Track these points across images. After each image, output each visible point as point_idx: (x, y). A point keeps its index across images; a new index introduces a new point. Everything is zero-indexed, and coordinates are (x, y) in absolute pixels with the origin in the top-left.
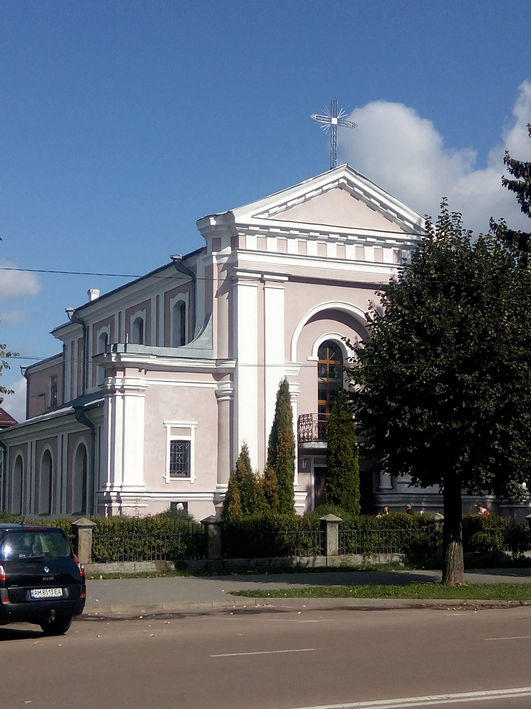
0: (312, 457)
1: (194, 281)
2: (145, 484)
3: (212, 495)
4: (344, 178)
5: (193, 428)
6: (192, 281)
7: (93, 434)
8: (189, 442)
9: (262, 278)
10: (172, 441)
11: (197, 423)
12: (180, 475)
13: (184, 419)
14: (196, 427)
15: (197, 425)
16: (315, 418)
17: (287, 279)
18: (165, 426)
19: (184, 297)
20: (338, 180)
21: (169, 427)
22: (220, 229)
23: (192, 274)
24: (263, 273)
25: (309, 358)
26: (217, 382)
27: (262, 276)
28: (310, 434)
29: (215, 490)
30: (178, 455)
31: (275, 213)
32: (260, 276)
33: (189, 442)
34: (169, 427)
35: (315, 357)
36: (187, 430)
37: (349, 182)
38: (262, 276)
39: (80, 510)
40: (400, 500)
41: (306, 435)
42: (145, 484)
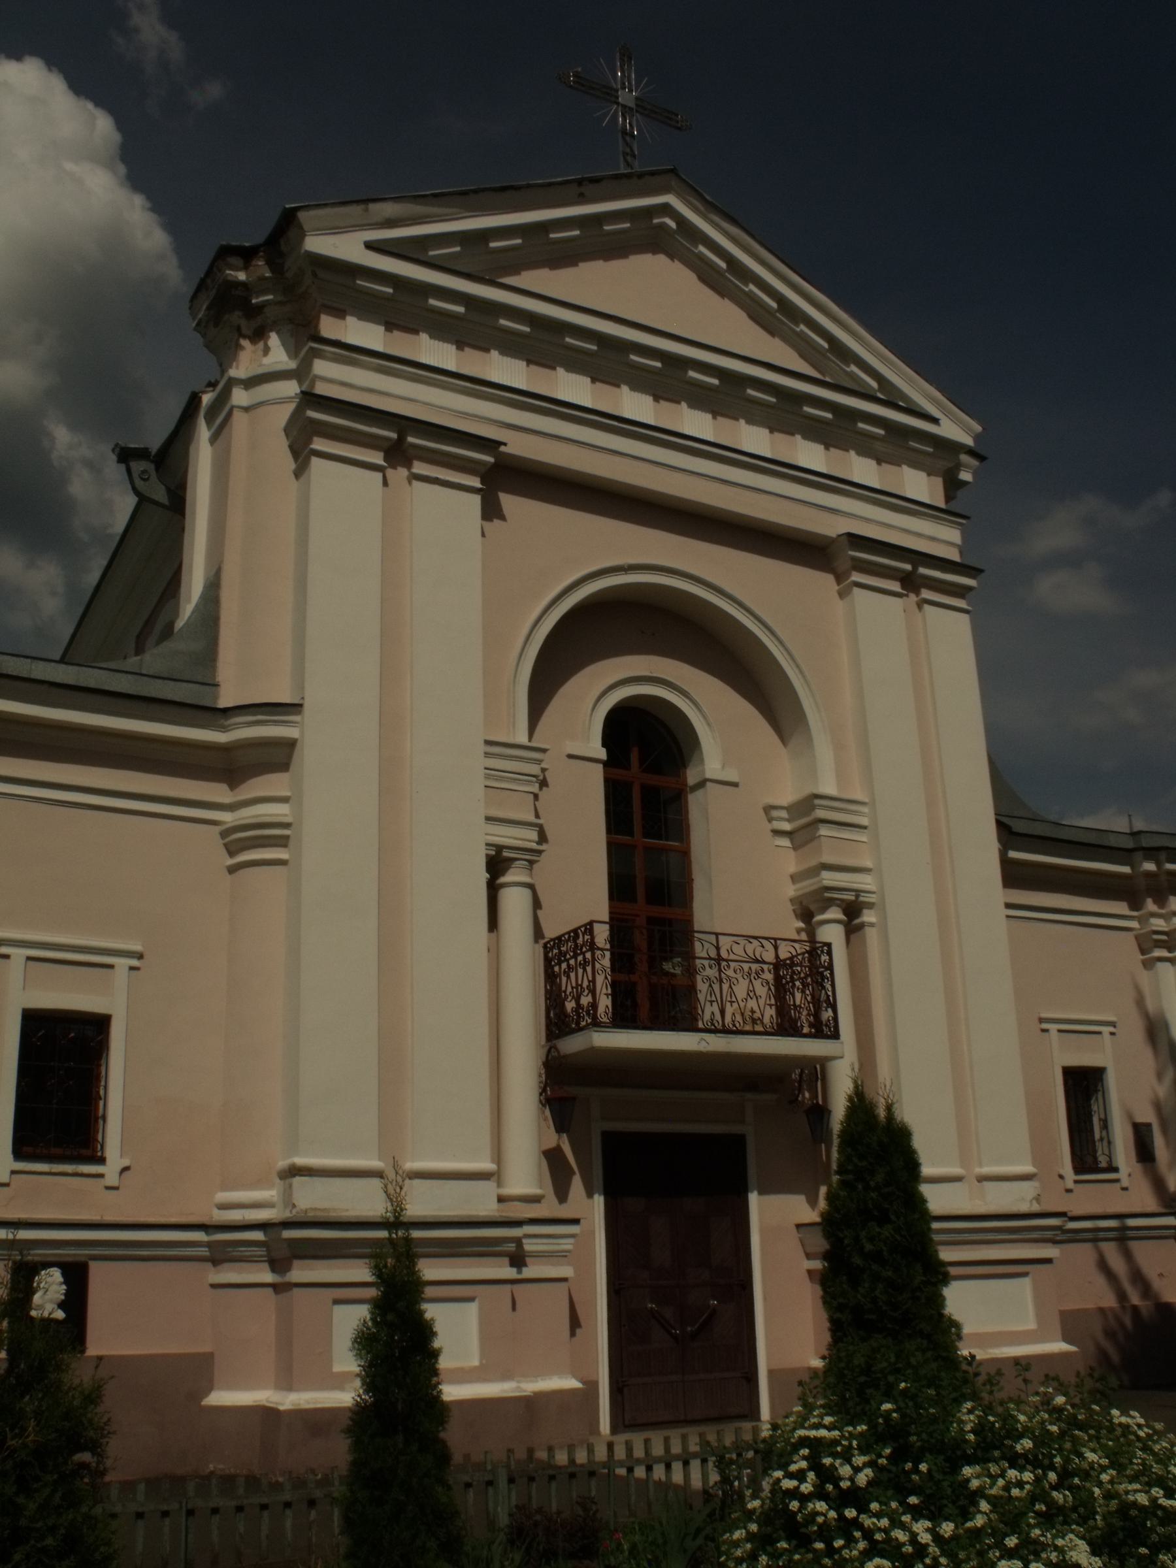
4: (666, 209)
8: (101, 1023)
15: (140, 956)
16: (602, 934)
27: (401, 439)
28: (586, 1000)
33: (101, 1023)
37: (681, 221)
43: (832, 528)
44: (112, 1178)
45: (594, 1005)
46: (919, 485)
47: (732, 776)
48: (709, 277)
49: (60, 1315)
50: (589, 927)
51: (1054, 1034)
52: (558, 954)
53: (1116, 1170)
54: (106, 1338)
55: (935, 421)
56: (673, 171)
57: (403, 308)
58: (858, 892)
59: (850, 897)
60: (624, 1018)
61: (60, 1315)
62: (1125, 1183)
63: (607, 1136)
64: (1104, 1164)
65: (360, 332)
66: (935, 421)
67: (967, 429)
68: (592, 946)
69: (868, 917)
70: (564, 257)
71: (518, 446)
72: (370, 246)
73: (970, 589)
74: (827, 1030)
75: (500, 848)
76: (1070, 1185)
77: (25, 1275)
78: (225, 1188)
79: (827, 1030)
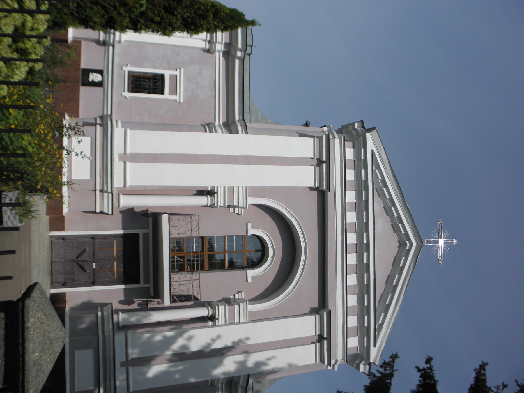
0: (150, 231)
3: (109, 113)
4: (411, 245)
5: (177, 98)
8: (162, 93)
9: (322, 162)
10: (162, 77)
11: (182, 101)
12: (130, 82)
13: (185, 90)
14: (178, 101)
18: (178, 70)
21: (177, 73)
22: (353, 131)
25: (249, 225)
26: (221, 123)
27: (324, 162)
29: (114, 116)
30: (150, 82)
33: (162, 93)
34: (177, 73)
35: (251, 232)
36: (174, 92)
37: (409, 251)
40: (106, 334)
43: (331, 306)
46: (353, 342)
47: (250, 280)
48: (396, 261)
49: (90, 79)
54: (84, 91)
55: (375, 346)
57: (360, 164)
58: (218, 319)
59: (217, 316)
61: (90, 79)
63: (137, 235)
65: (350, 154)
66: (375, 346)
67: (376, 359)
69: (210, 323)
70: (388, 212)
71: (330, 195)
72: (372, 151)
73: (323, 363)
77: (100, 72)
78: (122, 122)
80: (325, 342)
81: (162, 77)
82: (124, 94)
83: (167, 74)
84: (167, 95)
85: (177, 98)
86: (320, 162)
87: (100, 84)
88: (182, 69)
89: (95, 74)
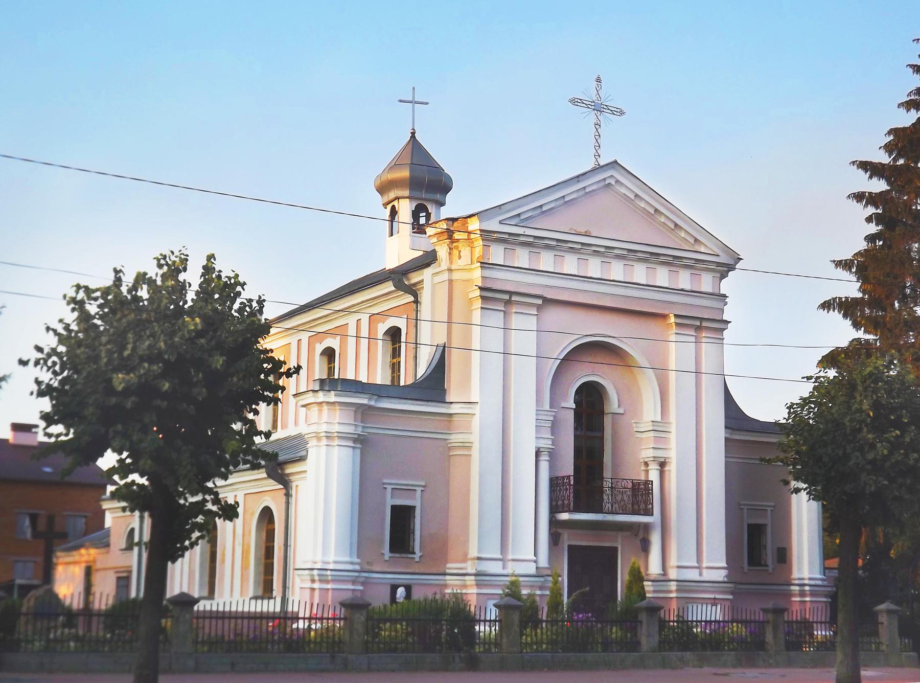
1: (416, 302)
2: (359, 561)
4: (612, 176)
6: (414, 302)
7: (288, 495)
10: (394, 508)
11: (423, 484)
15: (424, 486)
17: (540, 302)
19: (401, 323)
20: (605, 179)
23: (413, 291)
24: (511, 293)
27: (510, 297)
28: (566, 502)
31: (526, 219)
32: (507, 297)
34: (389, 488)
38: (510, 297)
39: (260, 593)
41: (560, 503)
42: (359, 561)
44: (417, 559)
45: (569, 504)
47: (621, 411)
50: (569, 477)
51: (745, 511)
52: (555, 483)
53: (767, 566)
56: (616, 162)
59: (662, 460)
60: (577, 509)
62: (771, 571)
63: (569, 546)
64: (763, 563)
68: (570, 484)
74: (649, 513)
75: (539, 448)
76: (746, 571)
77: (394, 588)
79: (649, 513)
80: (705, 324)
81: (394, 508)
82: (417, 559)
83: (390, 502)
84: (416, 502)
85: (419, 489)
86: (508, 303)
87: (408, 588)
88: (385, 481)
89: (398, 595)
